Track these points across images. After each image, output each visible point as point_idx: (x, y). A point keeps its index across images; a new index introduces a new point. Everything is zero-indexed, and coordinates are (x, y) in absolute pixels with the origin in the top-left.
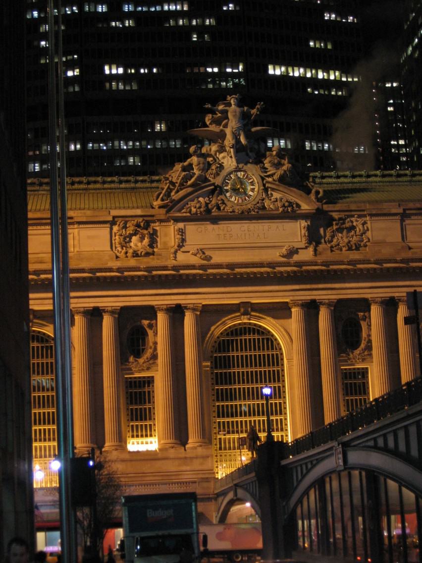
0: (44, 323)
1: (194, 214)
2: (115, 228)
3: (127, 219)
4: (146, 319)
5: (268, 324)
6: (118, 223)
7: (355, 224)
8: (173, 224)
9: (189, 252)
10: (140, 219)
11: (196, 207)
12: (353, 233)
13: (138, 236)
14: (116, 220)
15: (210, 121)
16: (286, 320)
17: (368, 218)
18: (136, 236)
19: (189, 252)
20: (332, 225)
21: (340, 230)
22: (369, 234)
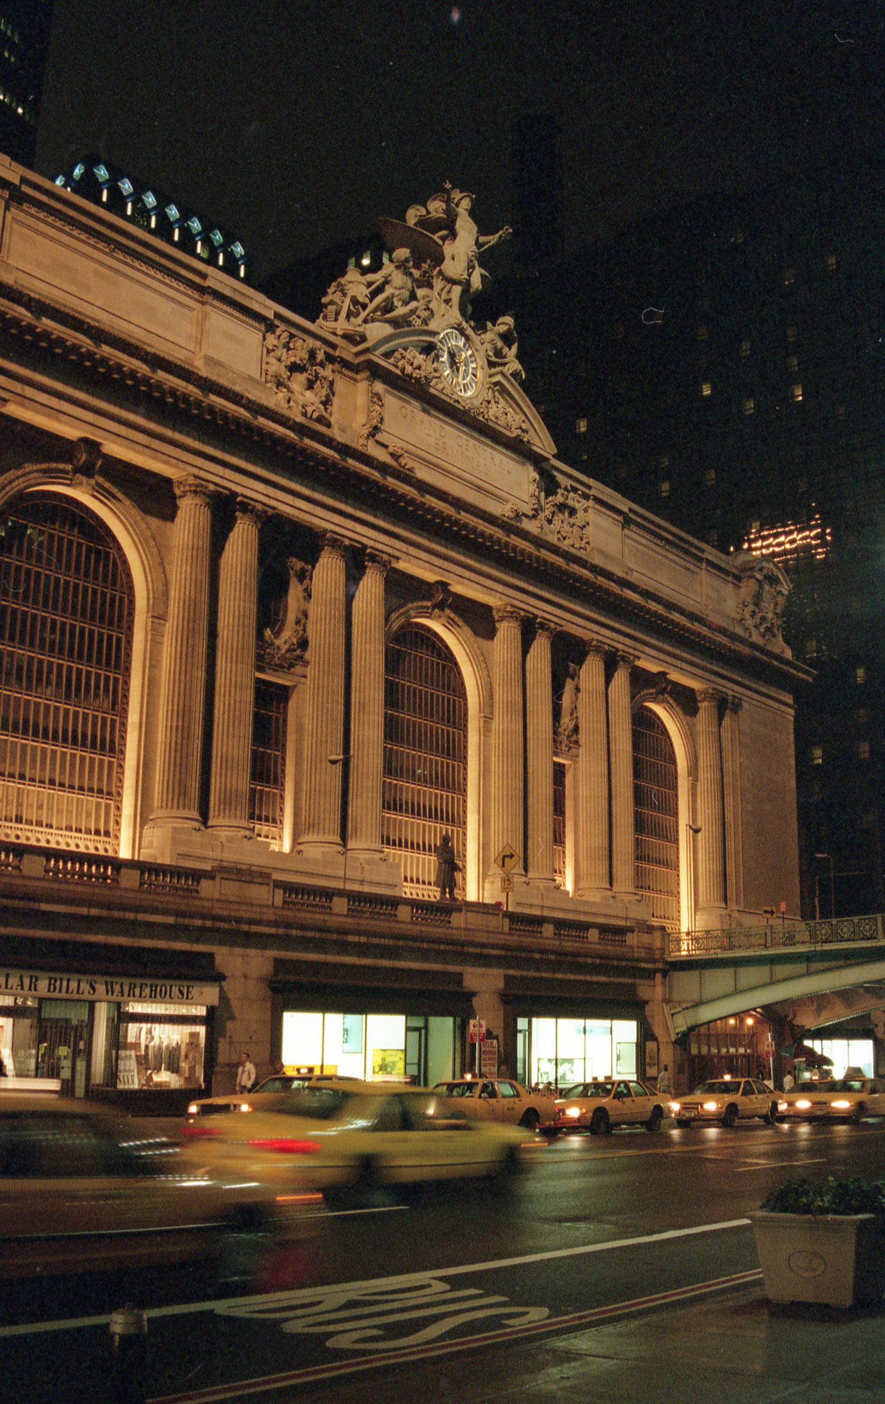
0: (114, 490)
1: (407, 375)
2: (271, 339)
3: (294, 331)
4: (300, 558)
5: (455, 641)
6: (278, 332)
7: (577, 506)
8: (367, 379)
9: (386, 447)
10: (318, 344)
11: (412, 364)
12: (572, 520)
13: (305, 375)
14: (277, 322)
15: (416, 220)
16: (485, 641)
17: (591, 503)
18: (302, 373)
19: (386, 447)
20: (555, 493)
21: (561, 507)
22: (589, 530)
